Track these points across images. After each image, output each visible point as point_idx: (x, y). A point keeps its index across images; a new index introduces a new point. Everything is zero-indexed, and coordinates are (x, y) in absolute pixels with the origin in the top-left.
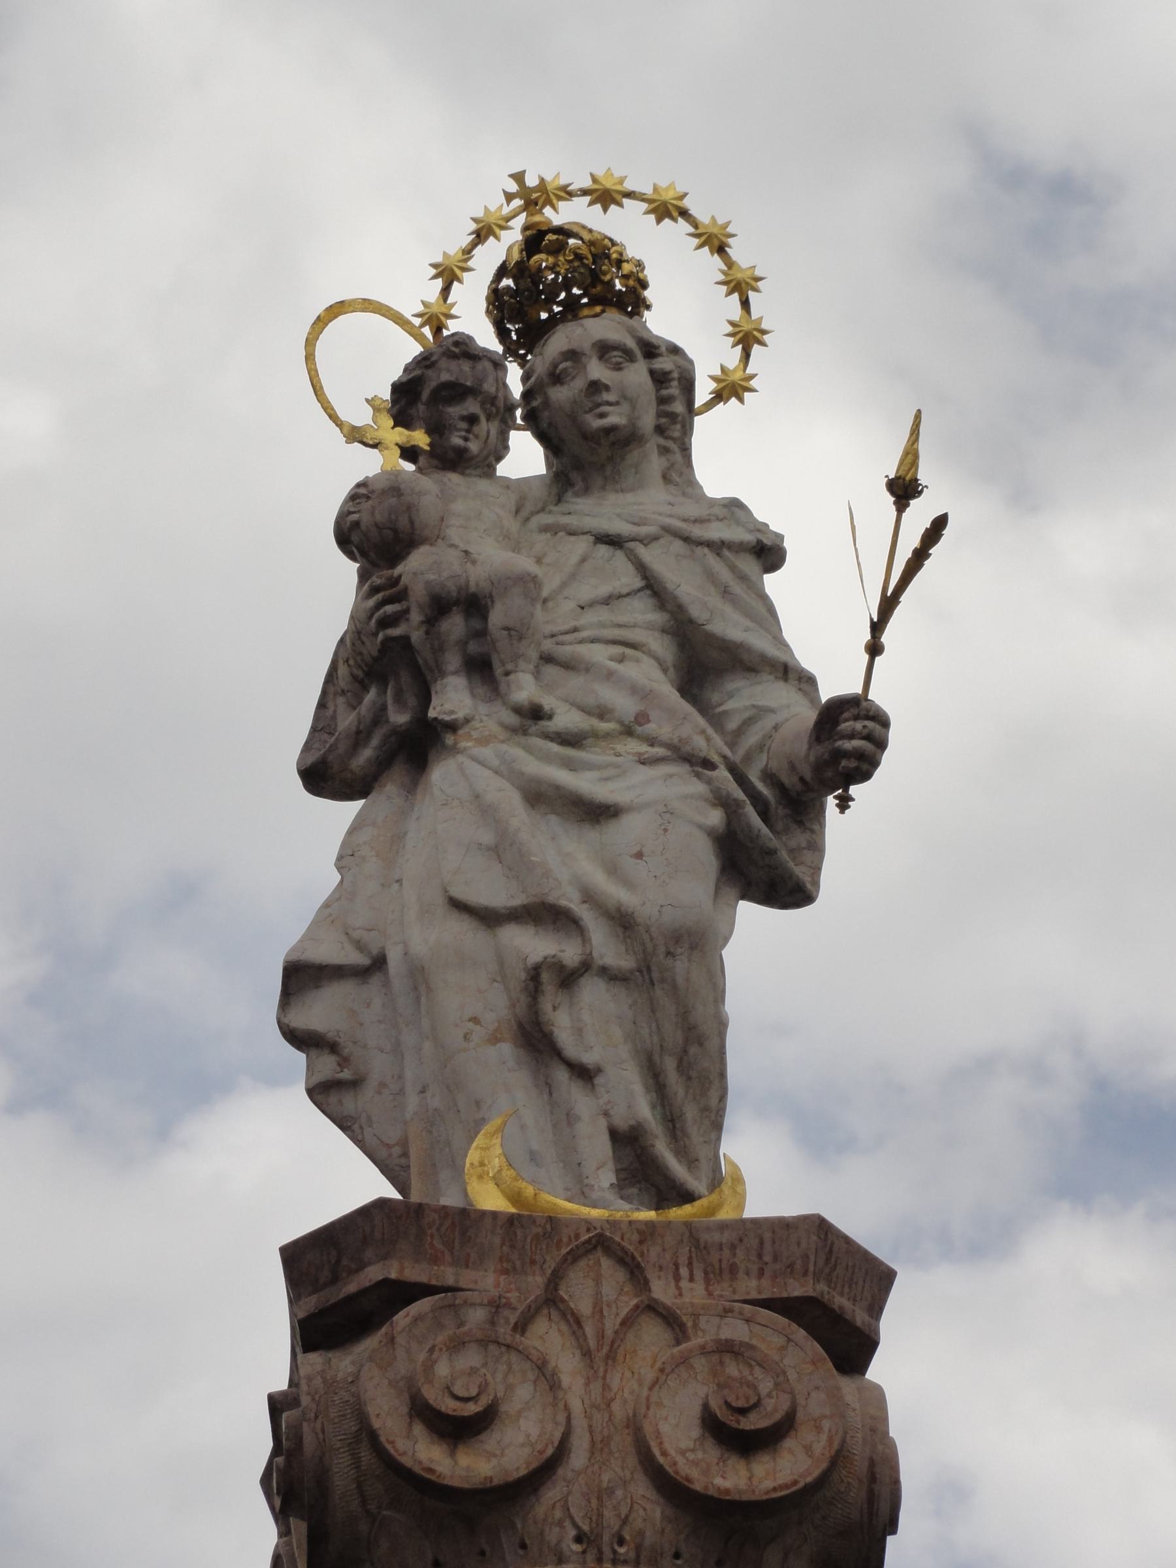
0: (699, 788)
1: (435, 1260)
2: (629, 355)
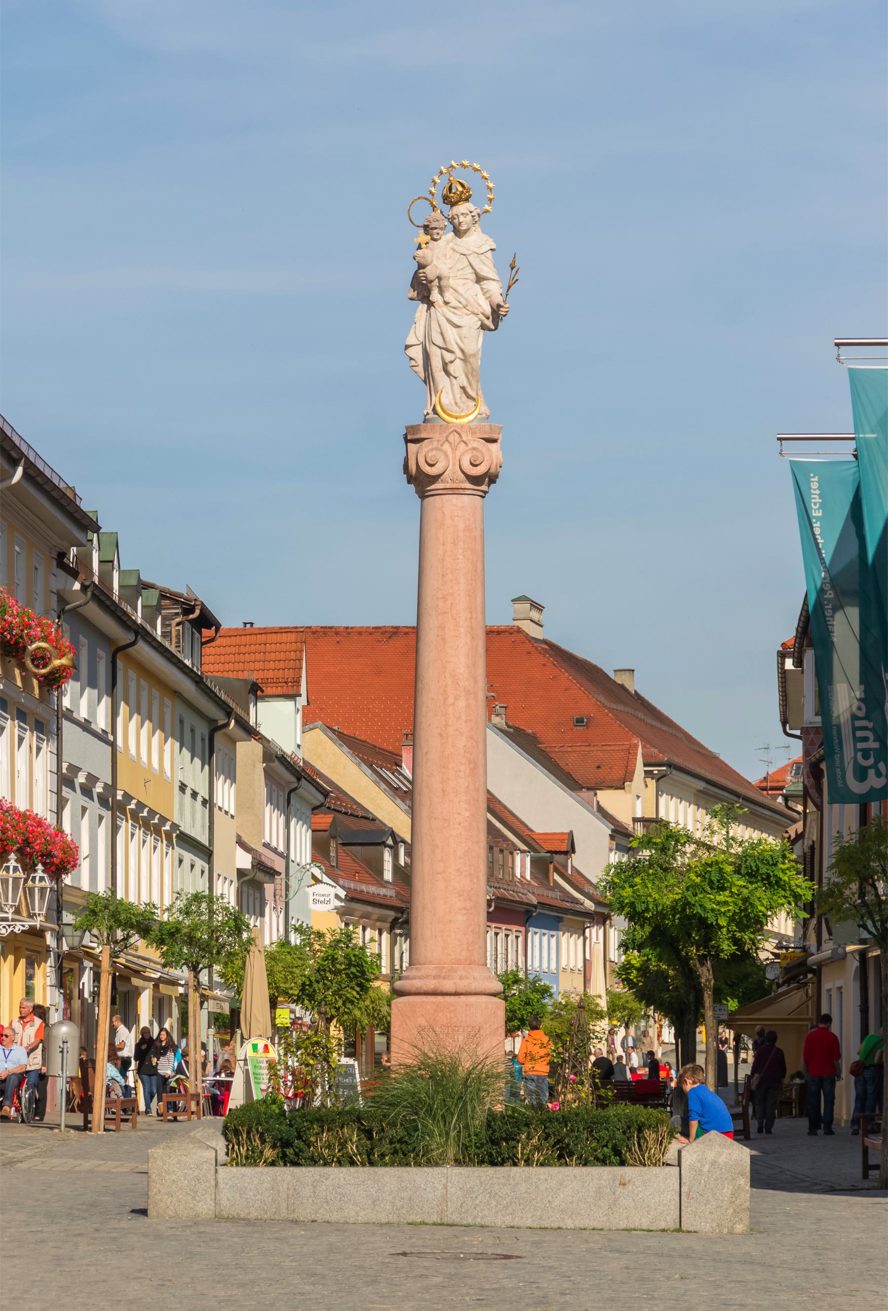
0: (476, 319)
1: (429, 433)
2: (467, 214)
